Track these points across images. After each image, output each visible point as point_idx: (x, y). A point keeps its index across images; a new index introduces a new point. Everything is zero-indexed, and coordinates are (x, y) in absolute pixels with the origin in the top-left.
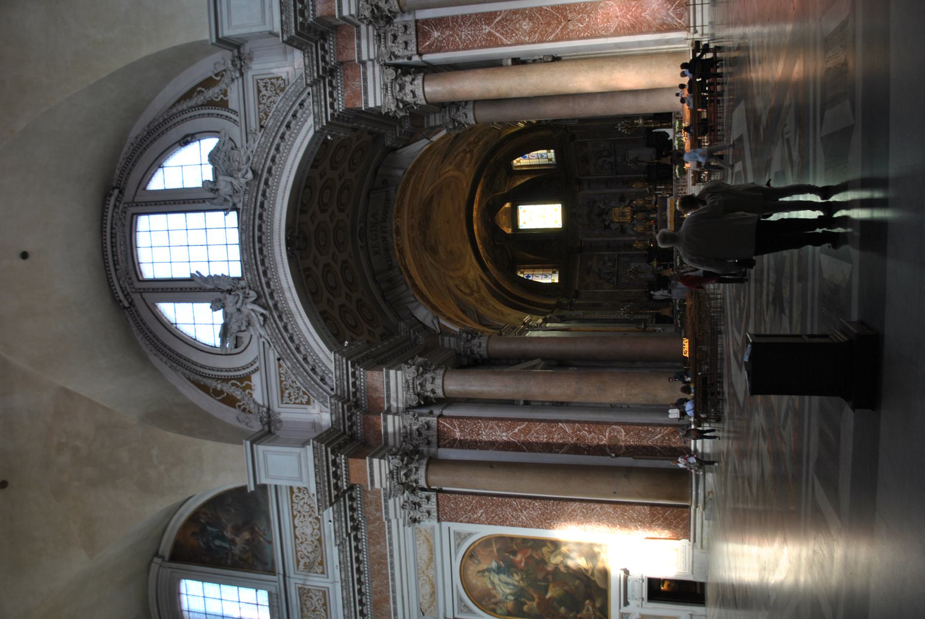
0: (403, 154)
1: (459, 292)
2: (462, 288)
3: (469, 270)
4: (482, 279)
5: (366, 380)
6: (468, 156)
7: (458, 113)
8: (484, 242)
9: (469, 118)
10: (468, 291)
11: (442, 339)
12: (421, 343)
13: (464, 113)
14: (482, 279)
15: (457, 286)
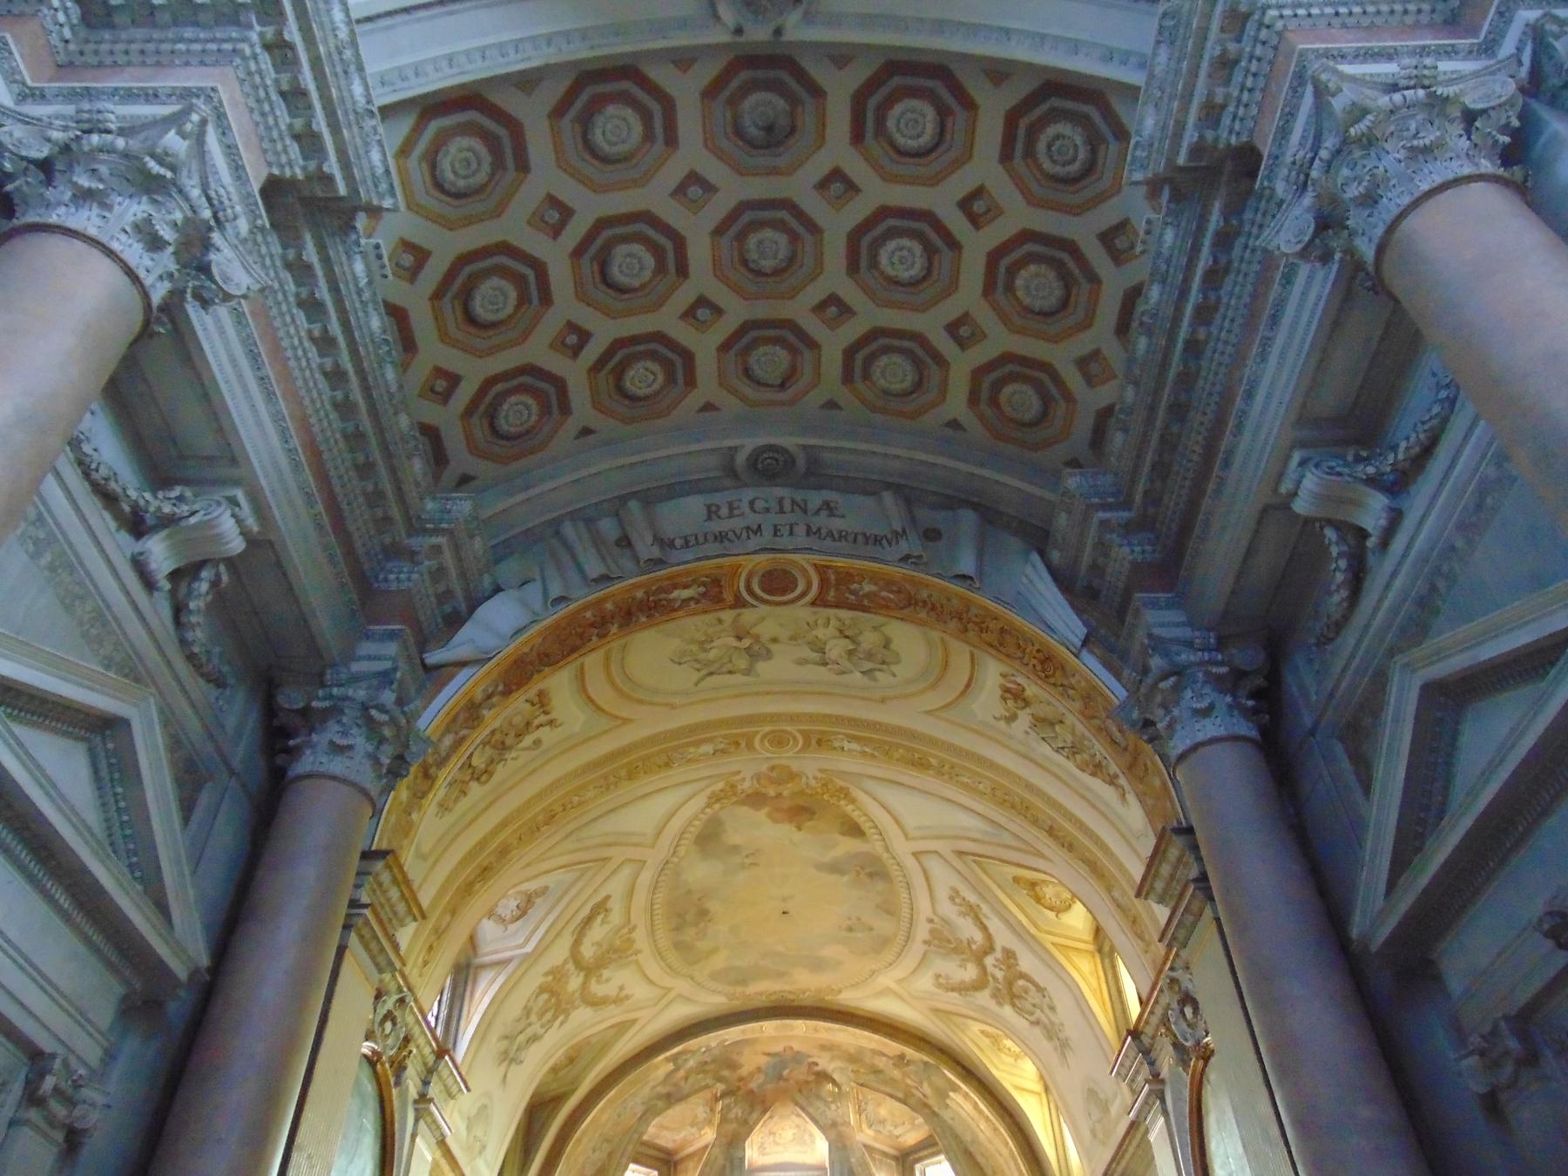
0: (1029, 570)
1: (586, 911)
2: (597, 932)
3: (651, 982)
4: (622, 1028)
5: (194, 61)
6: (970, 973)
7: (1207, 690)
8: (726, 1061)
9: (1198, 726)
10: (588, 951)
11: (392, 636)
12: (392, 577)
13: (1211, 707)
14: (622, 1028)
15: (601, 908)
